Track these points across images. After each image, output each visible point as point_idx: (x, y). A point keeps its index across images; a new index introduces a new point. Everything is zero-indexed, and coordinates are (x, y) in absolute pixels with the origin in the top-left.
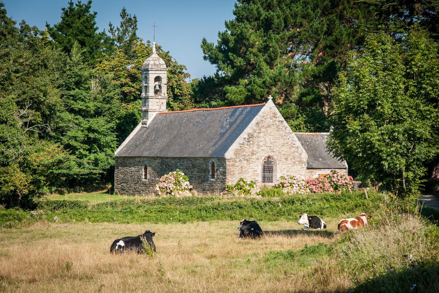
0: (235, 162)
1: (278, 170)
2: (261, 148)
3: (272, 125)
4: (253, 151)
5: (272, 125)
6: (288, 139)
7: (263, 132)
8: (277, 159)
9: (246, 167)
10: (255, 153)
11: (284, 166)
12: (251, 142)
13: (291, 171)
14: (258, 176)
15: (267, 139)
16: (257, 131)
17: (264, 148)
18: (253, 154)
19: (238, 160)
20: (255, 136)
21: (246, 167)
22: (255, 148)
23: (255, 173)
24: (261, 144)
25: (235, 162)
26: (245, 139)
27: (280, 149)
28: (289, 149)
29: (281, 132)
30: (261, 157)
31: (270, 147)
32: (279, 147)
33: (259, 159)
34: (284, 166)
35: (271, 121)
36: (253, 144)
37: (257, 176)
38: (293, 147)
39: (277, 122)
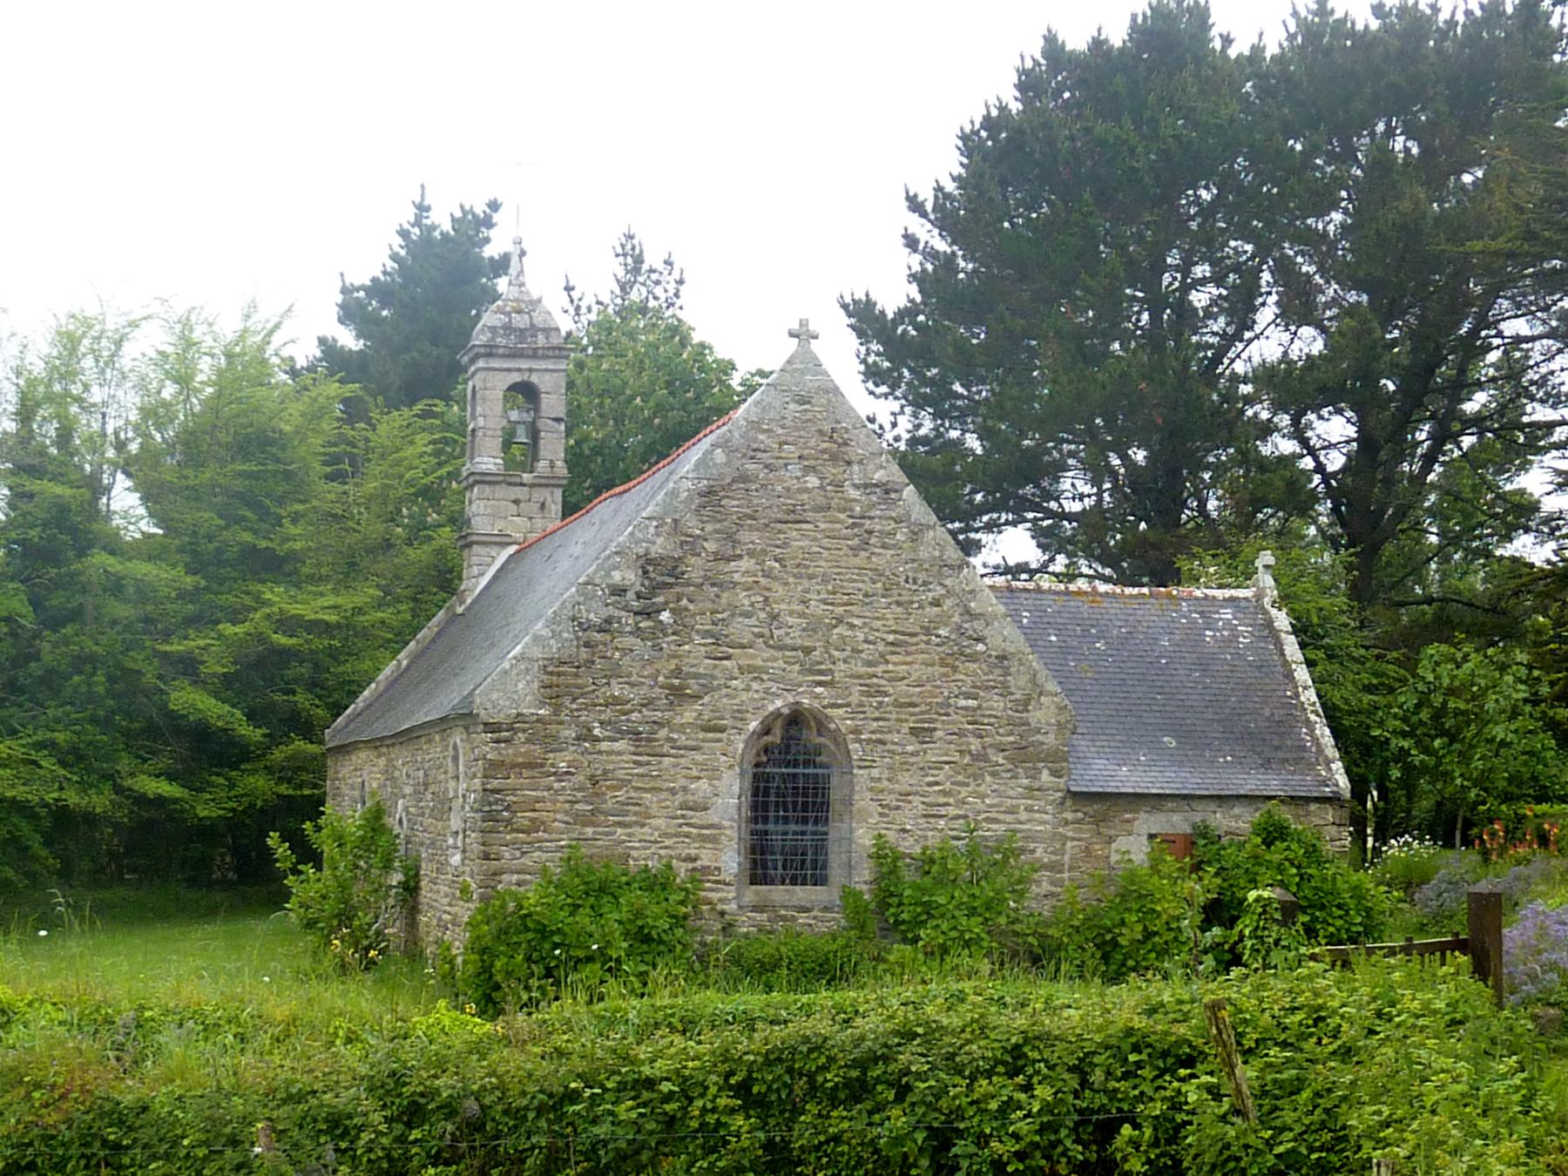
0: (552, 743)
1: (863, 800)
2: (742, 658)
3: (818, 509)
4: (677, 672)
5: (818, 509)
6: (936, 603)
7: (751, 554)
8: (856, 731)
9: (624, 783)
10: (693, 686)
11: (906, 780)
12: (665, 616)
13: (952, 811)
14: (714, 840)
15: (784, 598)
16: (711, 546)
17: (760, 656)
18: (678, 695)
19: (570, 733)
20: (695, 575)
21: (624, 783)
22: (696, 653)
23: (697, 817)
24: (741, 629)
25: (552, 743)
26: (619, 591)
27: (880, 669)
28: (938, 670)
29: (884, 558)
30: (740, 715)
31: (808, 651)
32: (869, 651)
33: (722, 730)
34: (906, 780)
35: (813, 481)
36: (682, 628)
37: (704, 838)
38: (973, 658)
39: (854, 494)
